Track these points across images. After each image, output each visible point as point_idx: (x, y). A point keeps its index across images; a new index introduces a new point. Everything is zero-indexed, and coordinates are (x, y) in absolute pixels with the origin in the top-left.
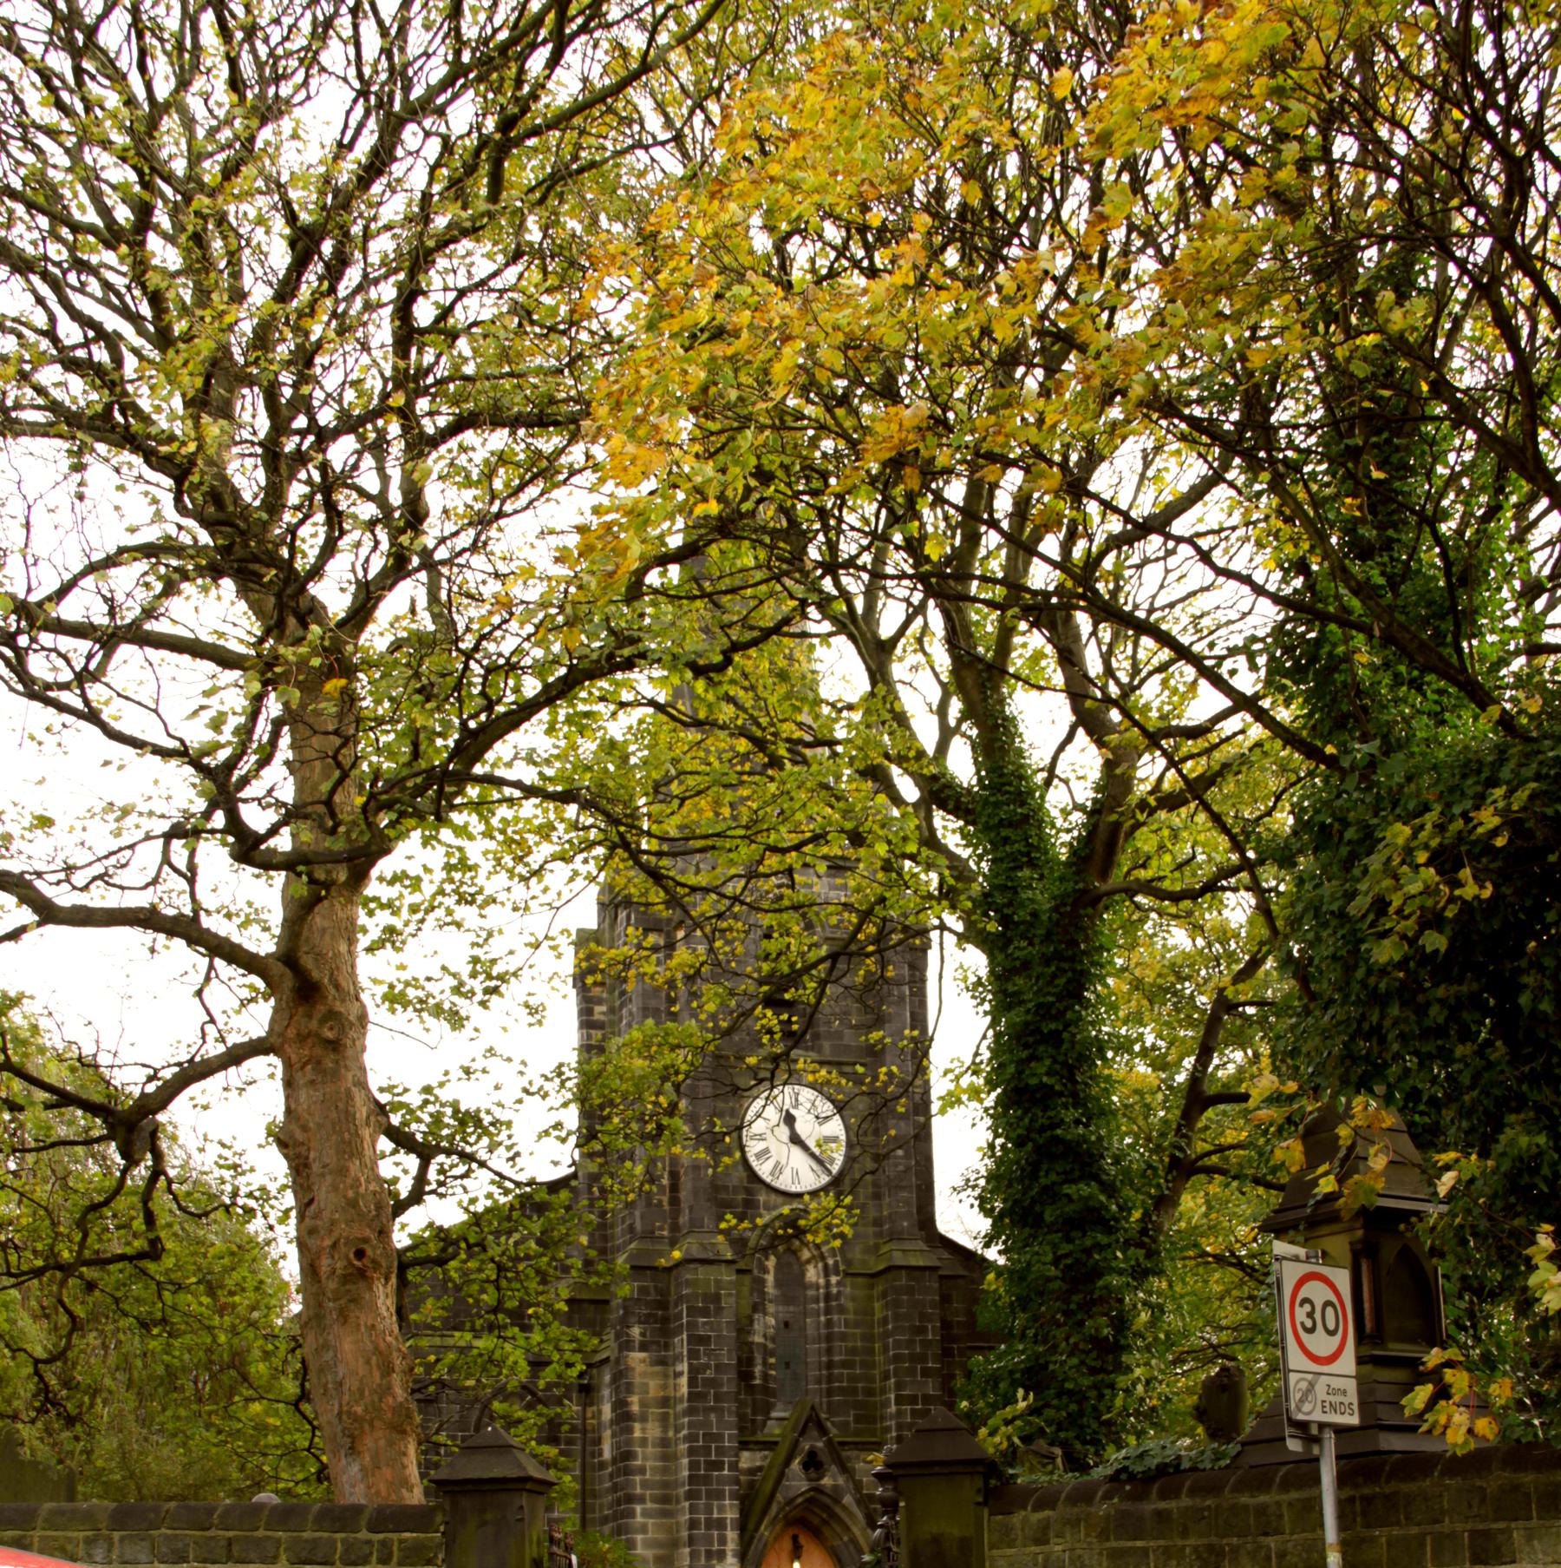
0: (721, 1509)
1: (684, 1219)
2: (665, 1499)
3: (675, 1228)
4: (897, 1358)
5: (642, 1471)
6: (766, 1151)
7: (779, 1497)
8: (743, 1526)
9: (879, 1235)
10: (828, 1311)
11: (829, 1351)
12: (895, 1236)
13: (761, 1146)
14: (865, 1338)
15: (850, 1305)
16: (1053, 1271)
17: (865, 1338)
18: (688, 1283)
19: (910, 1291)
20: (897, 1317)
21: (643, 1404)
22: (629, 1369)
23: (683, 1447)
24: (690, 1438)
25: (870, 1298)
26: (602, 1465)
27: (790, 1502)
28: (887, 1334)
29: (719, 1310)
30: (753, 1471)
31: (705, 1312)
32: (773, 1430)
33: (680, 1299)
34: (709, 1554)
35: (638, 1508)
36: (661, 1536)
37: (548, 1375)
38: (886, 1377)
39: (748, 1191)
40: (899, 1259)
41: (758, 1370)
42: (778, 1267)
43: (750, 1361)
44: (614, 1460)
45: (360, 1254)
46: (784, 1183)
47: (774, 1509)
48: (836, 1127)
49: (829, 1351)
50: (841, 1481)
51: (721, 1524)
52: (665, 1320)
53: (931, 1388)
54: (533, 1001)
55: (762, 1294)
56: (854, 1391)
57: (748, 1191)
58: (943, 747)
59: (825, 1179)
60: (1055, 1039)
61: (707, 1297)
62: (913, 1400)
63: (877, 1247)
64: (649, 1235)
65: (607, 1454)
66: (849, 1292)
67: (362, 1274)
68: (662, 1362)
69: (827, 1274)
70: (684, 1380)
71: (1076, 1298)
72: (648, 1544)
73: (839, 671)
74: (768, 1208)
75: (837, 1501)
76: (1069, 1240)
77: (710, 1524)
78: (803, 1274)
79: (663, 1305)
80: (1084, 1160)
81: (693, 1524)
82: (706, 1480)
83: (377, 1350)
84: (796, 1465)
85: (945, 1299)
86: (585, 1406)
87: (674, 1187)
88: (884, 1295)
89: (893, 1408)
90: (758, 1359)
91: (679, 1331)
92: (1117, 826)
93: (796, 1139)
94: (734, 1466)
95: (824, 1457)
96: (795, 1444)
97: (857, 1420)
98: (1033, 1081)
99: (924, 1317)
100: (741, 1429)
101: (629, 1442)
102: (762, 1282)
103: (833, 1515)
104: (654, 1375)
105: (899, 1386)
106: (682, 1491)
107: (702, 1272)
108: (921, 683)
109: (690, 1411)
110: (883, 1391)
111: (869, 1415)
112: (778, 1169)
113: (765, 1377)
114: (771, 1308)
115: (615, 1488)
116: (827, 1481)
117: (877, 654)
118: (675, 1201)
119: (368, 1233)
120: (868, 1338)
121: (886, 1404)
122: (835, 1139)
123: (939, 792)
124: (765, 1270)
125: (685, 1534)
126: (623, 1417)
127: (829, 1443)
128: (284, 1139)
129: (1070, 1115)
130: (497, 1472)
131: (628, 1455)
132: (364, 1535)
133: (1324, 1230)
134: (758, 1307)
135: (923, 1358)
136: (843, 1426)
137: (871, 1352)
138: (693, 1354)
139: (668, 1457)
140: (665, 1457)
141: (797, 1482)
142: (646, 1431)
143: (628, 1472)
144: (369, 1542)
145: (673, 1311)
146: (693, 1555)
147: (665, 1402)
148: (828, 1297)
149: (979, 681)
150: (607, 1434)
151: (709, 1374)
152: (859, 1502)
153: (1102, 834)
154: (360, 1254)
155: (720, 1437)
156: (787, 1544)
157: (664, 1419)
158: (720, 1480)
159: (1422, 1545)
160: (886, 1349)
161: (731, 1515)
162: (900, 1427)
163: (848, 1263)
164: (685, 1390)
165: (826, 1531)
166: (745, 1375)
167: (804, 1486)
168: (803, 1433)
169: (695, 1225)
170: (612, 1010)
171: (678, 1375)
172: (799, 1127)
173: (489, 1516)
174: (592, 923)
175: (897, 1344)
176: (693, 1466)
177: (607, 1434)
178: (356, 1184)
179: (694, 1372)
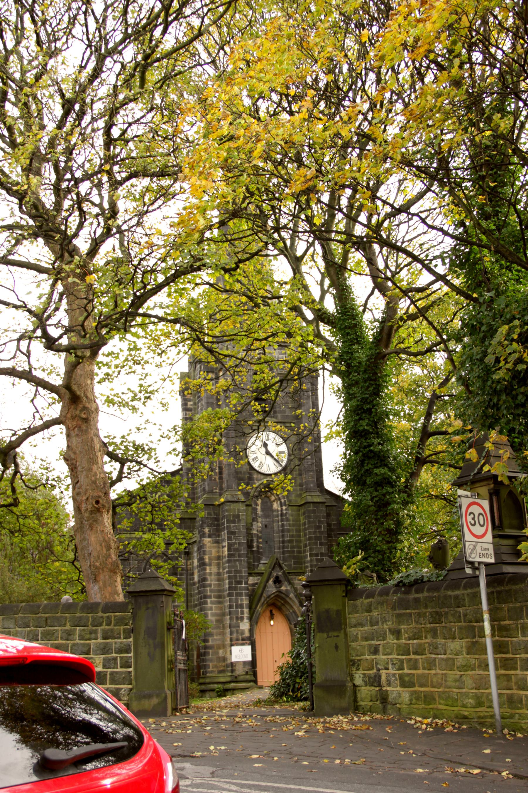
0: (242, 600)
1: (225, 485)
2: (219, 597)
3: (221, 489)
4: (310, 539)
5: (210, 585)
6: (256, 458)
7: (264, 595)
8: (250, 607)
9: (302, 490)
11: (283, 536)
12: (308, 490)
13: (255, 456)
15: (291, 518)
16: (371, 503)
18: (227, 511)
19: (314, 511)
20: (309, 522)
21: (210, 559)
22: (204, 545)
23: (226, 576)
24: (229, 572)
25: (299, 515)
26: (194, 584)
27: (269, 597)
28: (305, 529)
29: (239, 521)
30: (254, 585)
31: (234, 522)
32: (261, 568)
33: (224, 517)
34: (237, 618)
35: (209, 600)
36: (218, 612)
37: (172, 548)
38: (306, 546)
39: (250, 474)
40: (310, 499)
41: (255, 544)
42: (262, 503)
43: (252, 541)
44: (199, 582)
45: (97, 502)
46: (264, 470)
47: (263, 599)
48: (284, 448)
49: (283, 536)
50: (289, 588)
51: (241, 606)
52: (218, 525)
53: (324, 550)
54: (164, 402)
55: (256, 514)
56: (293, 552)
57: (250, 474)
58: (322, 298)
59: (280, 468)
60: (369, 411)
61: (234, 516)
62: (316, 555)
63: (301, 495)
64: (211, 492)
65: (196, 579)
66: (290, 512)
67: (98, 510)
68: (217, 542)
69: (281, 506)
70: (226, 549)
71: (380, 513)
72: (213, 615)
73: (281, 269)
74: (258, 480)
75: (287, 596)
76: (377, 491)
77: (237, 606)
78: (272, 506)
79: (217, 519)
80: (382, 459)
81: (231, 607)
82: (235, 589)
83: (105, 540)
84: (271, 582)
85: (328, 515)
86: (187, 560)
87: (221, 473)
88: (304, 513)
89: (309, 559)
91: (223, 529)
92: (391, 327)
93: (268, 453)
94: (246, 583)
95: (282, 578)
96: (271, 573)
98: (361, 428)
99: (320, 522)
100: (249, 568)
101: (205, 574)
102: (256, 509)
103: (286, 602)
104: (214, 547)
105: (311, 549)
106: (226, 593)
107: (232, 506)
108: (313, 273)
109: (229, 561)
110: (305, 552)
111: (299, 561)
112: (261, 464)
113: (258, 547)
114: (260, 520)
115: (199, 593)
116: (283, 588)
117: (296, 262)
118: (221, 478)
119: (100, 494)
120: (299, 531)
121: (306, 557)
122: (283, 453)
123: (321, 316)
124: (257, 505)
125: (227, 610)
126: (202, 564)
127: (284, 573)
128: (68, 458)
129: (376, 441)
130: (153, 588)
131: (204, 579)
132: (100, 614)
133: (478, 485)
134: (254, 519)
135: (320, 538)
136: (289, 566)
137: (299, 536)
138: (229, 539)
140: (219, 580)
141: (272, 589)
142: (211, 569)
143: (204, 586)
144: (102, 617)
145: (221, 522)
146: (231, 619)
147: (219, 558)
148: (282, 515)
149: (336, 271)
150: (196, 571)
151: (236, 546)
152: (296, 596)
153: (386, 330)
154: (97, 502)
155: (240, 571)
156: (268, 613)
157: (218, 565)
158: (241, 589)
159: (522, 611)
160: (305, 535)
161: (245, 602)
162: (311, 566)
163: (290, 501)
164: (226, 553)
165: (283, 608)
166: (250, 546)
167: (274, 590)
168: (273, 569)
169: (229, 488)
170: (195, 404)
171: (223, 547)
172: (269, 448)
173: (150, 605)
174: (186, 370)
175: (310, 533)
176: (230, 583)
177: (196, 571)
178: (96, 474)
179: (230, 545)
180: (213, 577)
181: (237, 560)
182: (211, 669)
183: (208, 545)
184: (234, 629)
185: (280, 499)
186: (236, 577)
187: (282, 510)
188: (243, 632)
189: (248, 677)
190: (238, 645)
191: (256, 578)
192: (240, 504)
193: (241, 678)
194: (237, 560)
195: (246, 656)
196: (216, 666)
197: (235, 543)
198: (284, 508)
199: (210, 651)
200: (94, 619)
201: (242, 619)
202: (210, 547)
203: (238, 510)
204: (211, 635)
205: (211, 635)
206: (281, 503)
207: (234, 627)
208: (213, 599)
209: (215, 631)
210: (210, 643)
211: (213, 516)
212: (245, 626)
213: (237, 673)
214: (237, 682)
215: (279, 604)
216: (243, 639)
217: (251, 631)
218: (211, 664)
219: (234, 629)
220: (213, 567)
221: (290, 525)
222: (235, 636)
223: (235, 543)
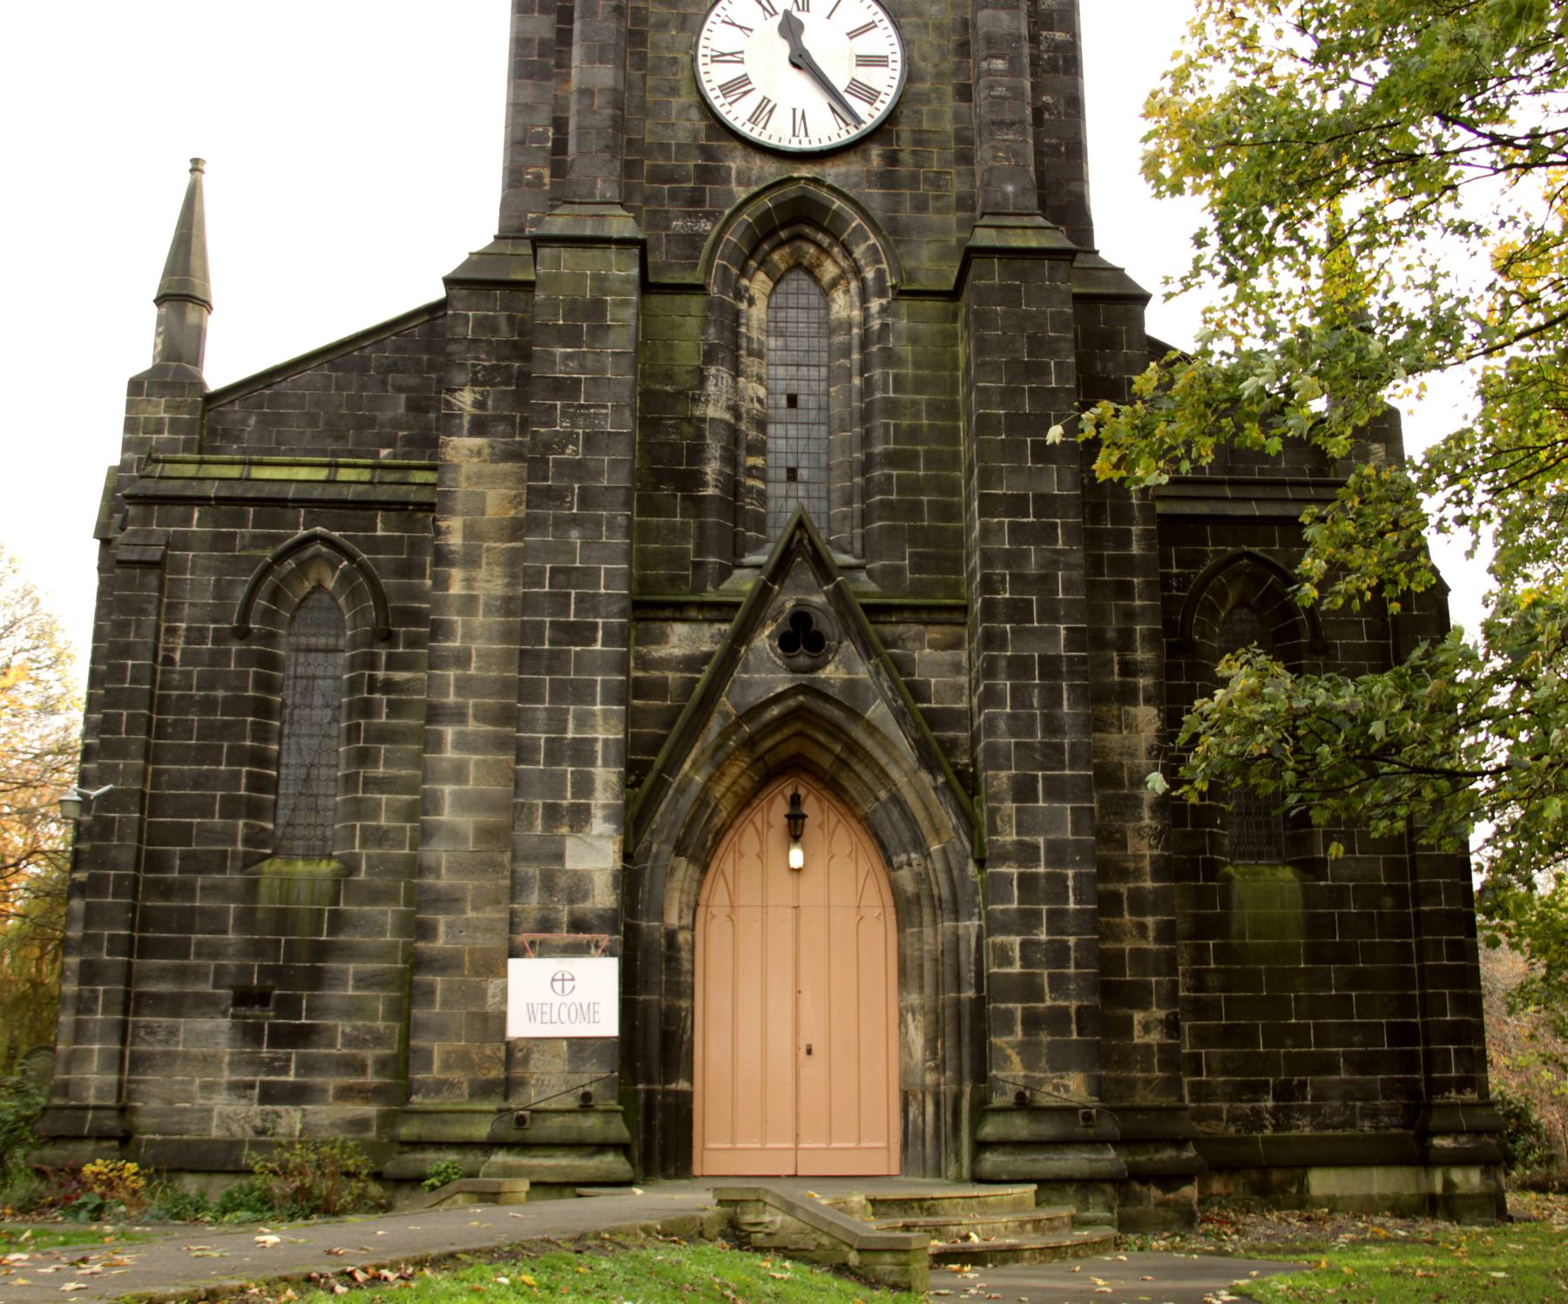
0: (584, 721)
5: (462, 659)
6: (744, 80)
7: (725, 703)
10: (864, 367)
11: (866, 440)
14: (935, 410)
15: (906, 350)
17: (935, 410)
19: (1010, 296)
21: (470, 532)
25: (950, 339)
29: (600, 330)
35: (449, 732)
39: (706, 152)
41: (712, 469)
46: (778, 134)
47: (714, 726)
49: (866, 440)
50: (863, 672)
51: (582, 752)
56: (914, 510)
61: (572, 308)
62: (1016, 505)
69: (864, 298)
72: (465, 803)
75: (856, 715)
82: (555, 662)
84: (764, 639)
90: (714, 449)
93: (801, 61)
95: (827, 625)
97: (919, 564)
99: (1036, 343)
103: (854, 748)
104: (494, 478)
105: (985, 480)
111: (941, 555)
116: (832, 673)
122: (879, 61)
127: (839, 597)
137: (952, 436)
141: (766, 672)
155: (589, 576)
167: (782, 682)
172: (808, 40)
180: (480, 619)
181: (574, 521)
182: (436, 1072)
183: (469, 466)
184: (532, 871)
185: (857, 271)
186: (560, 602)
187: (867, 317)
188: (579, 886)
189: (591, 1124)
190: (544, 950)
191: (708, 631)
192: (612, 253)
193: (553, 1127)
194: (574, 521)
195: (588, 1012)
196: (464, 1060)
197: (569, 438)
199: (439, 981)
200: (185, 857)
201: (580, 817)
202: (478, 477)
203: (597, 278)
204: (449, 901)
205: (449, 901)
207: (535, 858)
208: (472, 726)
209: (470, 884)
210: (441, 943)
211: (505, 333)
212: (595, 855)
213: (532, 1096)
214: (524, 1146)
215: (826, 761)
216: (578, 925)
217: (630, 879)
218: (437, 1049)
219: (532, 871)
220: (482, 573)
221: (899, 384)
222: (532, 902)
223: (569, 438)
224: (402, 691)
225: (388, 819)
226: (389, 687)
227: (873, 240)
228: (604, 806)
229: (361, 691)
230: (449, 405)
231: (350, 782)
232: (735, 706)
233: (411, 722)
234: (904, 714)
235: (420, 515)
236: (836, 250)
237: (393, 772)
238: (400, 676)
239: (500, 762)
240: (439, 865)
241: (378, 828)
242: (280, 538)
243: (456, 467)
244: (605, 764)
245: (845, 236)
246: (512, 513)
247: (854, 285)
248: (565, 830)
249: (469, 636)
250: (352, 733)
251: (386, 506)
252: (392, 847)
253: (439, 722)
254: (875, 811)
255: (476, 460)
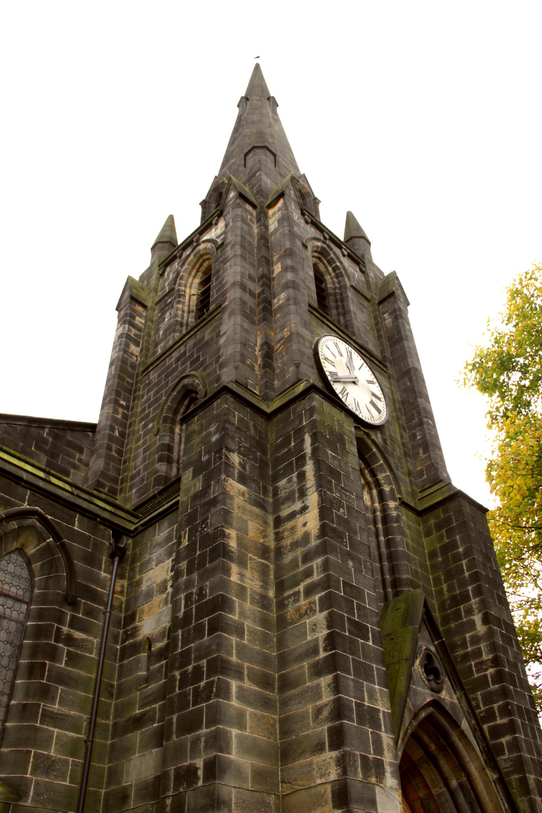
10: (387, 532)
11: (393, 570)
36: (261, 738)
49: (393, 570)
75: (456, 725)
139: (278, 621)
148: (386, 519)
185: (378, 484)
198: (392, 504)
202: (244, 510)
206: (381, 493)
208: (247, 684)
220: (248, 573)
224: (77, 647)
225: (56, 750)
226: (69, 640)
227: (388, 473)
228: (391, 764)
229: (49, 637)
230: (227, 458)
231: (26, 711)
232: (413, 706)
233: (82, 673)
234: (475, 729)
235: (102, 527)
236: (366, 471)
237: (65, 710)
238: (79, 635)
239: (264, 717)
240: (230, 800)
241: (48, 757)
242: (13, 505)
243: (232, 498)
244: (386, 732)
245: (375, 466)
246: (262, 540)
247: (375, 492)
248: (373, 780)
249: (242, 614)
250: (33, 671)
251: (84, 512)
252: (56, 777)
253: (228, 675)
254: (442, 793)
255: (242, 498)
